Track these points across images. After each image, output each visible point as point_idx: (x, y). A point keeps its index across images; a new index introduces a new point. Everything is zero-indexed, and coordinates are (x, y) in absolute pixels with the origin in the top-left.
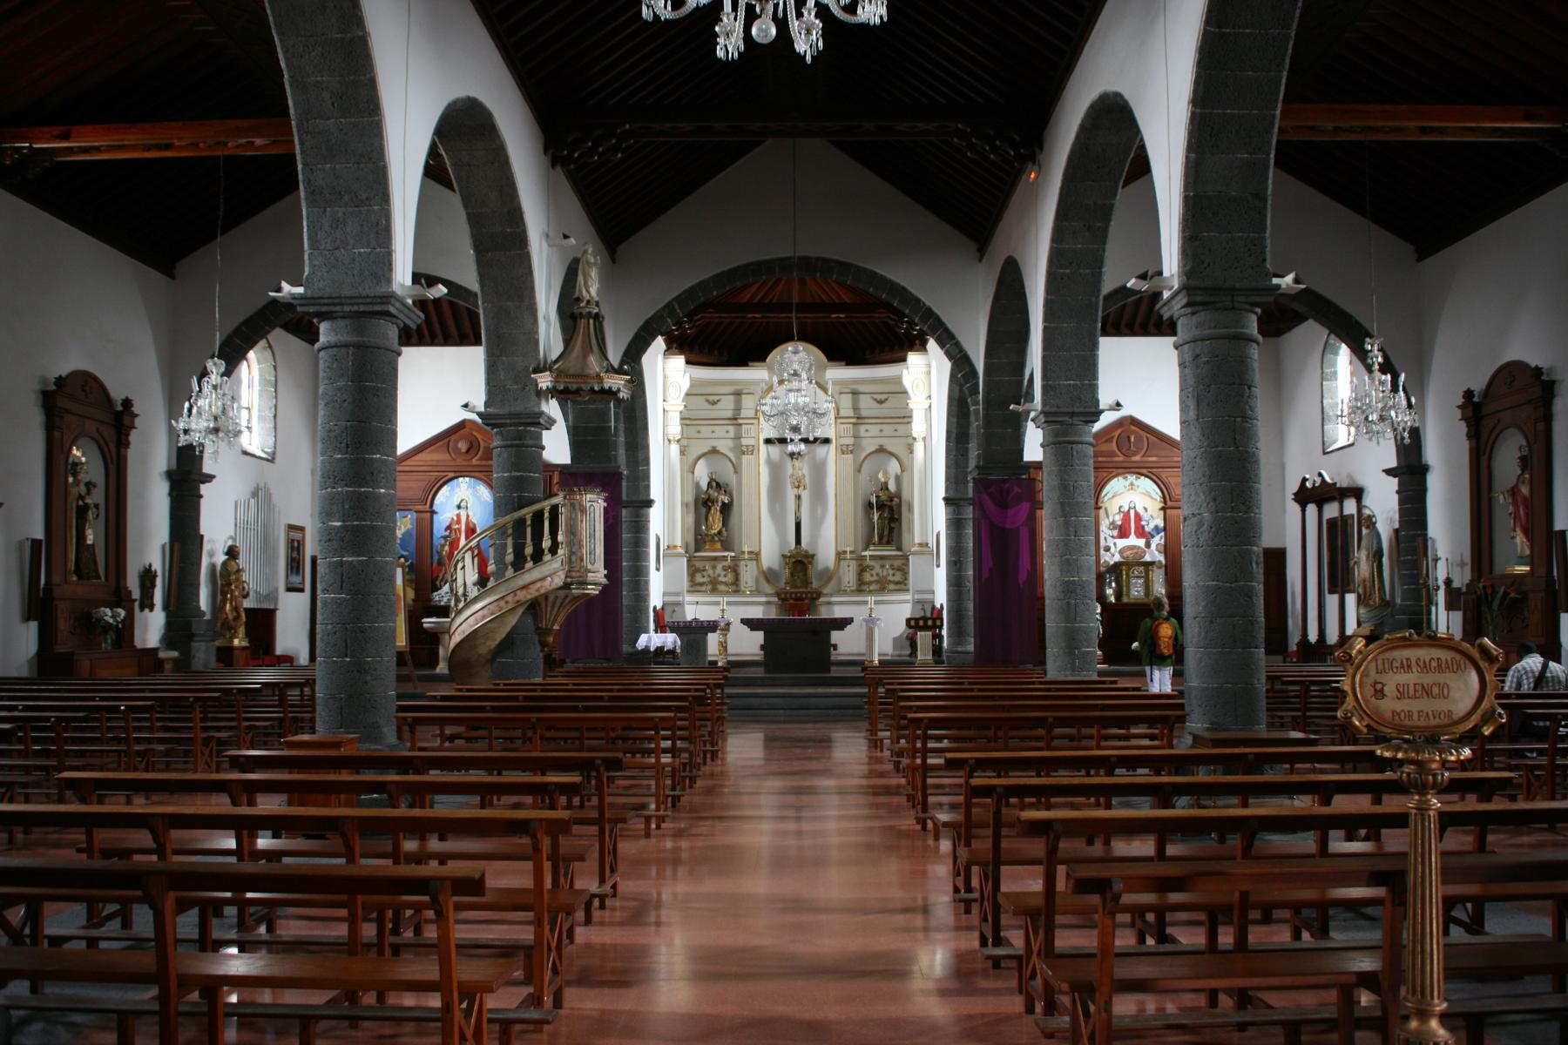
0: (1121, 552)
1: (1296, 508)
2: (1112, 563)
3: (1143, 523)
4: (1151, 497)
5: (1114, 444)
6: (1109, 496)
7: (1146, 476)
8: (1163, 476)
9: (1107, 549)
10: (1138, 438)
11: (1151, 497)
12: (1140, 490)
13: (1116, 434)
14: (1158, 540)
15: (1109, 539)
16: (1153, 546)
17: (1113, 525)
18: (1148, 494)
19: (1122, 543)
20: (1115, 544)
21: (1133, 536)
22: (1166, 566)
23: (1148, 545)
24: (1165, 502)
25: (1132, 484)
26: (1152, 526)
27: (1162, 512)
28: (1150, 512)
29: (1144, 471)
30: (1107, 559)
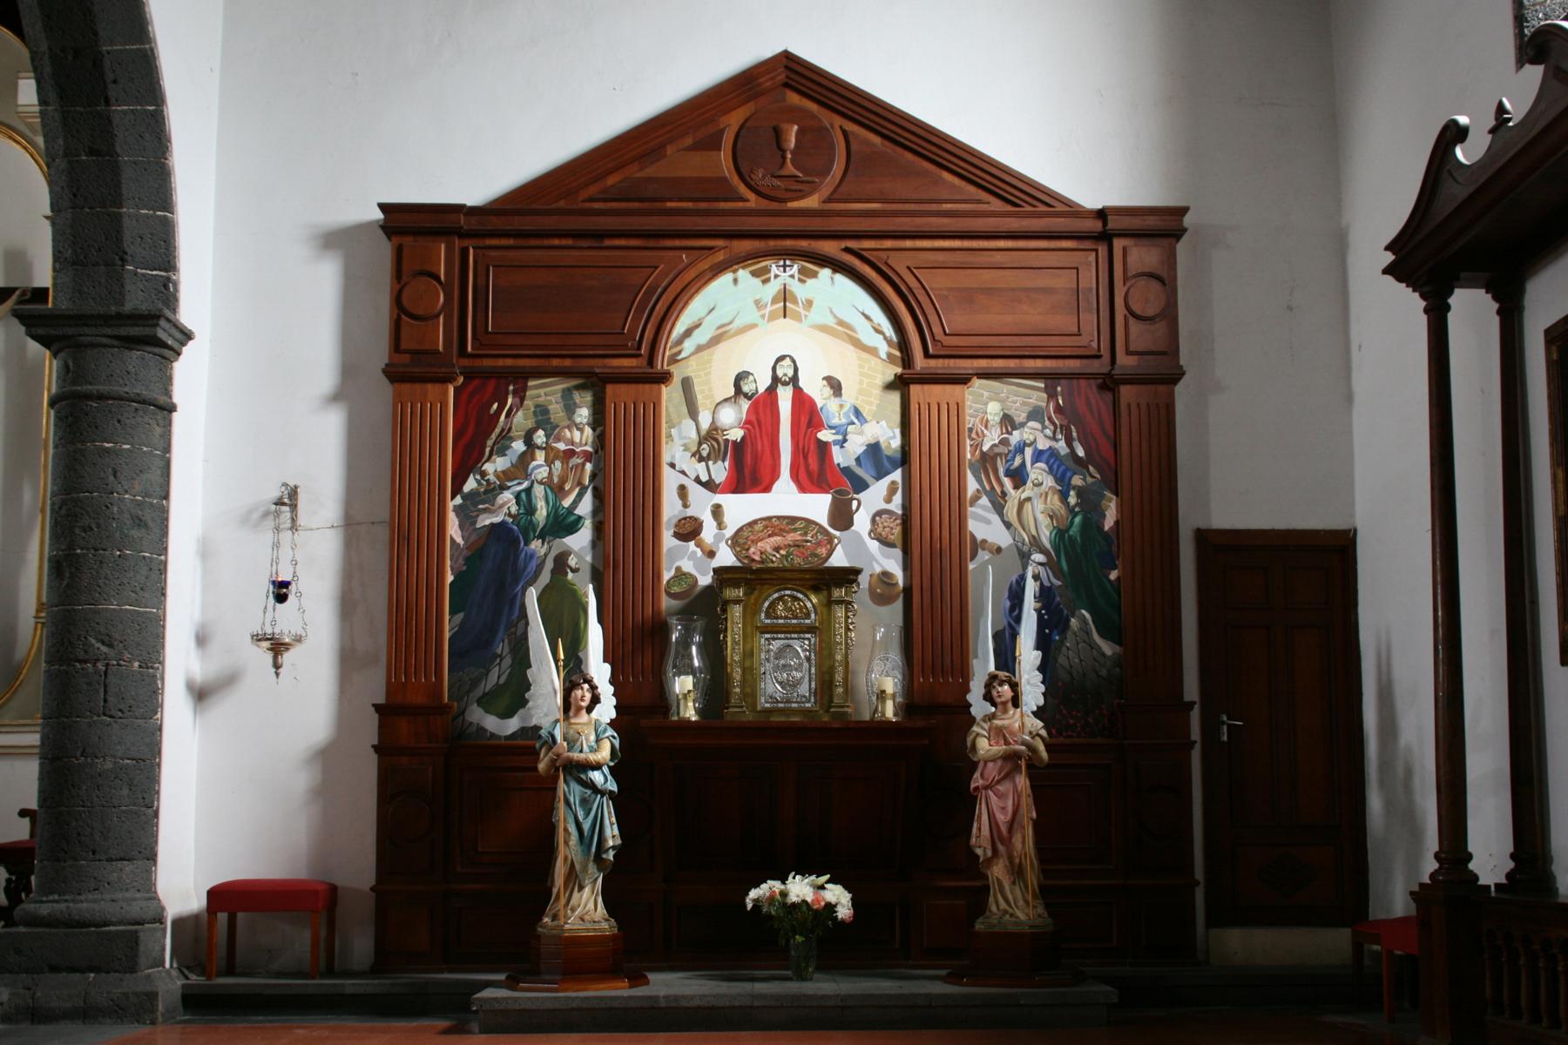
0: (737, 541)
1: (1409, 304)
2: (705, 580)
3: (825, 435)
4: (857, 344)
5: (725, 157)
6: (700, 337)
7: (838, 267)
8: (899, 263)
9: (689, 530)
10: (814, 137)
11: (857, 344)
12: (819, 315)
13: (733, 121)
14: (877, 498)
15: (696, 492)
16: (862, 522)
17: (711, 443)
18: (843, 331)
19: (743, 508)
20: (717, 511)
21: (785, 483)
22: (907, 591)
23: (842, 516)
24: (907, 360)
25: (785, 296)
26: (857, 444)
27: (895, 398)
28: (850, 395)
29: (830, 248)
30: (688, 566)
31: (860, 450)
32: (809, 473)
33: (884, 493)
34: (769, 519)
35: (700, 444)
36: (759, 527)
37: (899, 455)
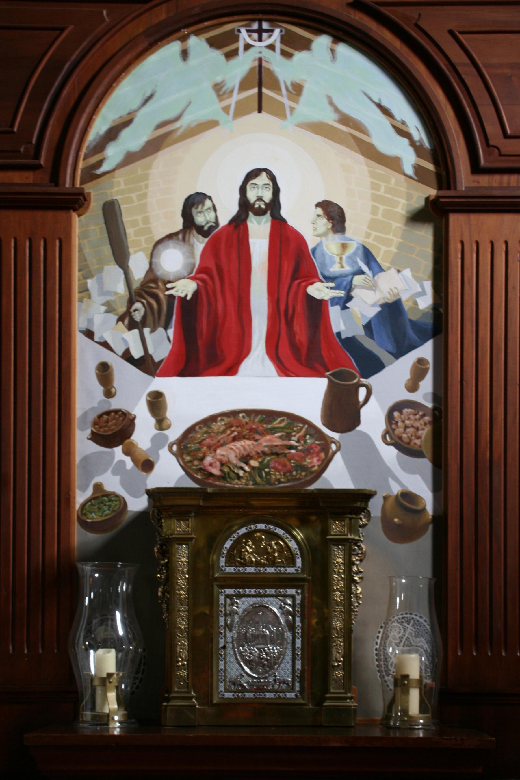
31: (372, 312)
32: (294, 347)
33: (407, 376)
34: (234, 413)
35: (131, 302)
36: (216, 426)
37: (429, 321)
